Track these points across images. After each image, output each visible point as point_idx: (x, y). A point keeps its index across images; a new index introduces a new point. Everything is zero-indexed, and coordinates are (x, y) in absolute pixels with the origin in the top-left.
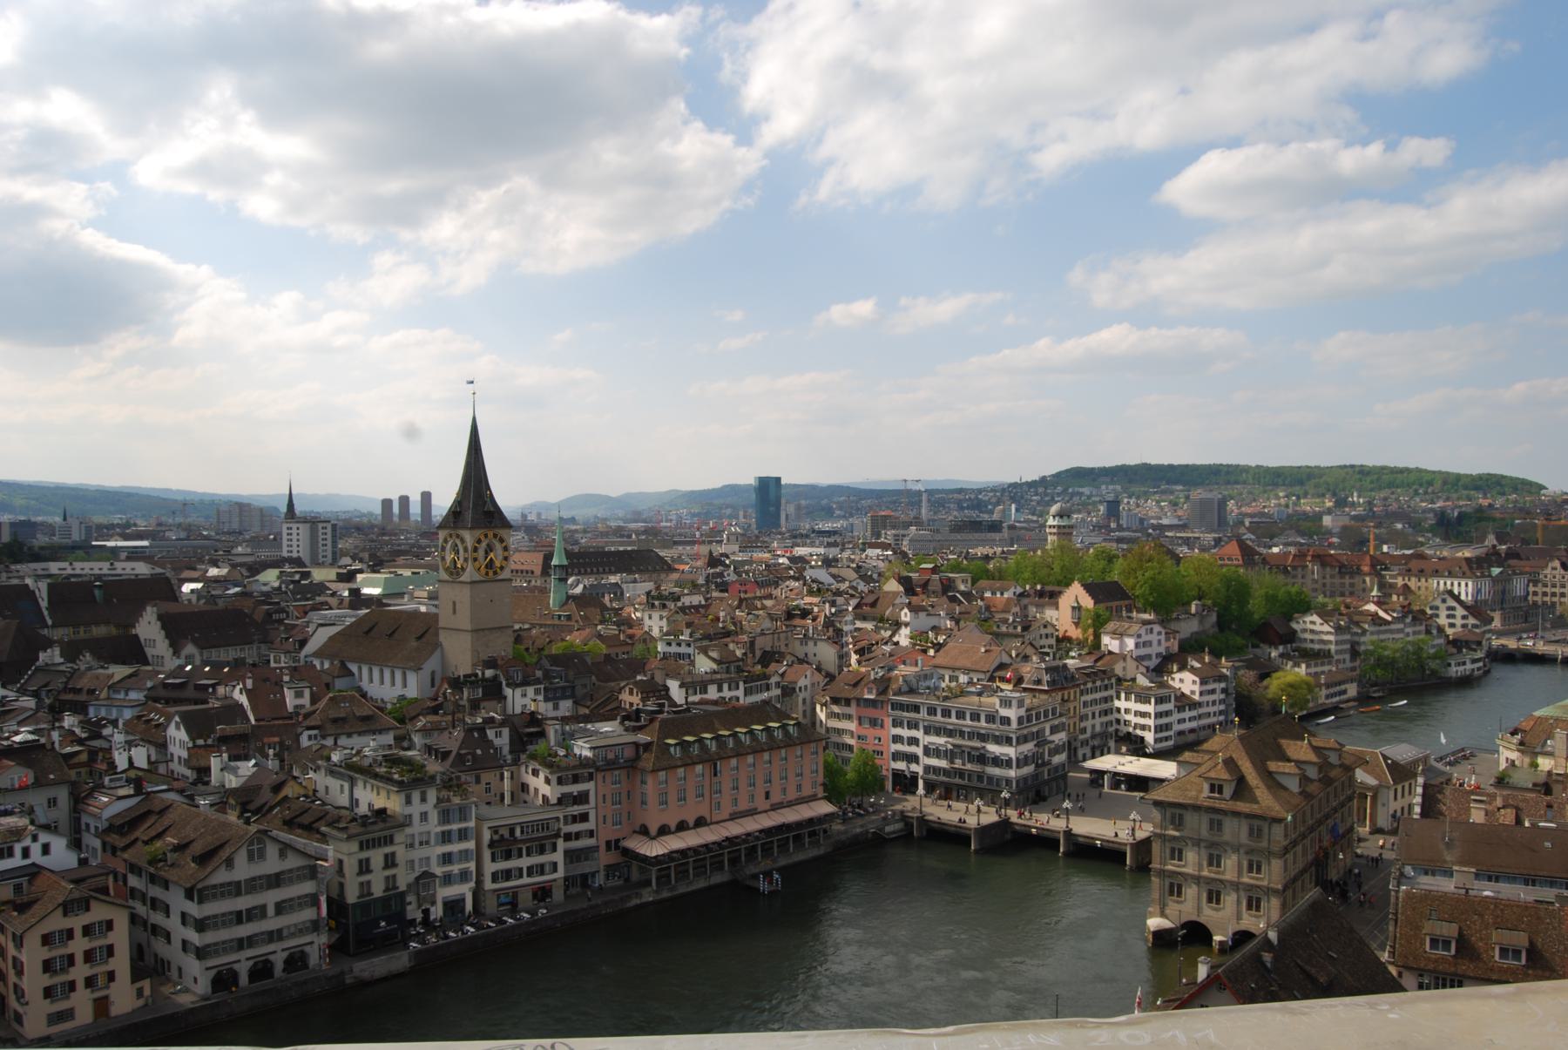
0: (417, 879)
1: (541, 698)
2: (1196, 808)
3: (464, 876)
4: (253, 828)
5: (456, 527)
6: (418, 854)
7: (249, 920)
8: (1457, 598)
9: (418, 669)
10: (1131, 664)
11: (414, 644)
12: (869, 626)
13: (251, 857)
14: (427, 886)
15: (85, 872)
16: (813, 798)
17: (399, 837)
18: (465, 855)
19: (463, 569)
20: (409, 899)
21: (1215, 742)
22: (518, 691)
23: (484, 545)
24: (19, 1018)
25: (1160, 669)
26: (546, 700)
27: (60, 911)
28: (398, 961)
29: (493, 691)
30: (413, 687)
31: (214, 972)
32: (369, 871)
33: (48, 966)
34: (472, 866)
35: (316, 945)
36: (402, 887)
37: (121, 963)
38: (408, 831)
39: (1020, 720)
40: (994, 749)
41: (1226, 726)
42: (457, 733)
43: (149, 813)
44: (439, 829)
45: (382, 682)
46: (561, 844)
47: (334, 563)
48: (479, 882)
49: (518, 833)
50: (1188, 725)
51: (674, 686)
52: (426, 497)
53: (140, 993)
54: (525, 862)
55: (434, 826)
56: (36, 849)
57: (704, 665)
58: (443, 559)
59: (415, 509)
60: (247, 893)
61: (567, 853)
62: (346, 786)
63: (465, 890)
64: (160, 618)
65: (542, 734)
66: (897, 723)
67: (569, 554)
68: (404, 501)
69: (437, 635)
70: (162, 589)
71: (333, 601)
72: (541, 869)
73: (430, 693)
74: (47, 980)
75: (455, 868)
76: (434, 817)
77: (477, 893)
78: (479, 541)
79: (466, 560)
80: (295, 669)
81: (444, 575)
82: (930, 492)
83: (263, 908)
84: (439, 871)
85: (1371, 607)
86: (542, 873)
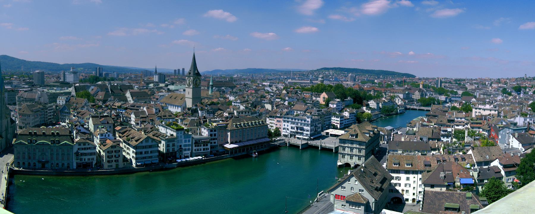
2: (348, 140)
3: (189, 149)
8: (400, 97)
9: (180, 106)
10: (335, 110)
12: (279, 100)
13: (146, 142)
15: (115, 141)
16: (265, 137)
21: (352, 126)
25: (341, 111)
30: (179, 110)
36: (176, 150)
39: (311, 122)
40: (305, 128)
41: (355, 123)
47: (164, 82)
48: (192, 151)
50: (347, 123)
51: (235, 112)
52: (183, 69)
57: (242, 108)
59: (181, 72)
64: (130, 93)
65: (206, 121)
66: (284, 121)
67: (213, 81)
68: (179, 70)
70: (131, 87)
75: (187, 148)
76: (183, 137)
81: (187, 86)
82: (293, 72)
85: (384, 99)
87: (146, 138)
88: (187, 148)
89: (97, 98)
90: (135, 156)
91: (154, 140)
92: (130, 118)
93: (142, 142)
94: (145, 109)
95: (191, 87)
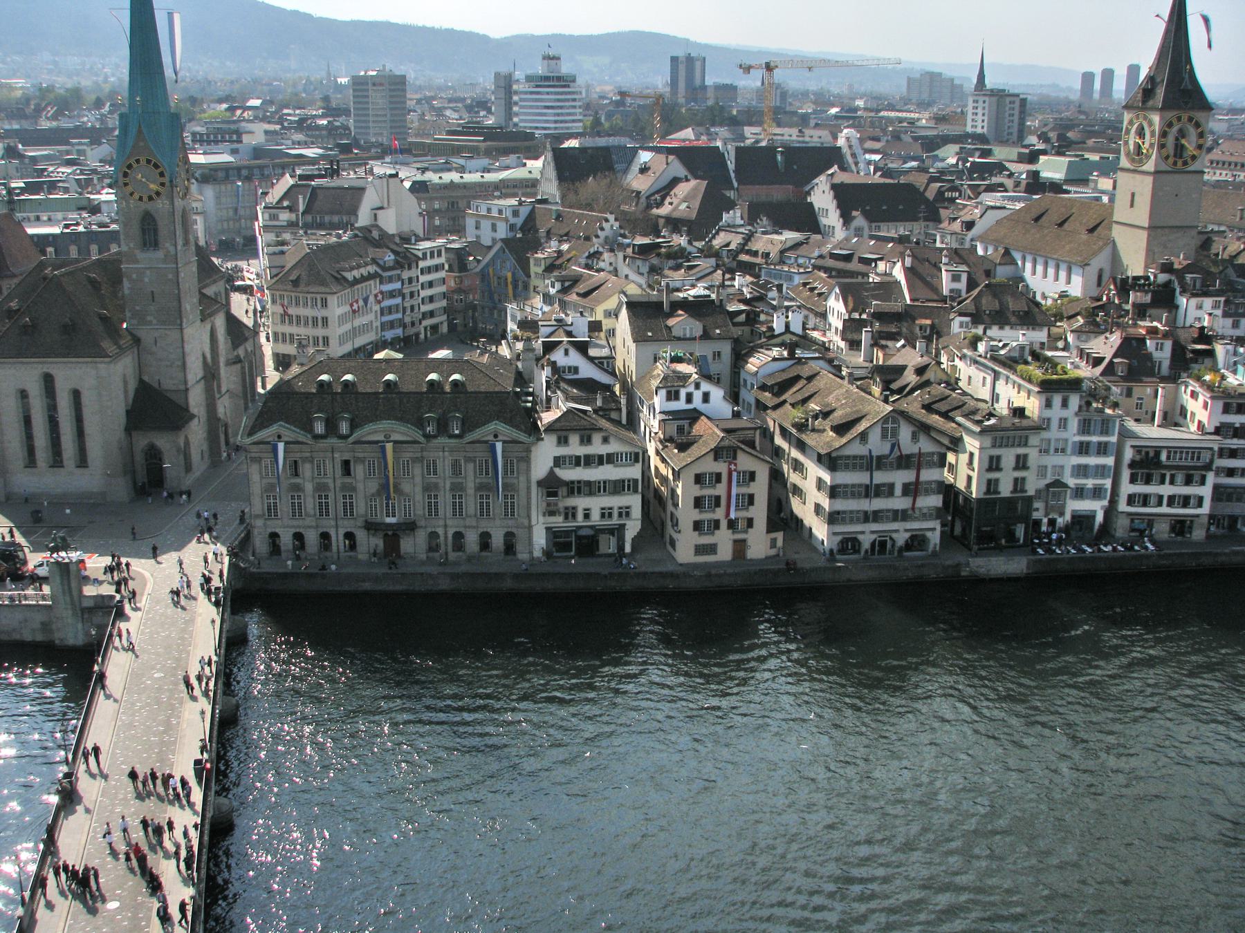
0: (1048, 486)
1: (1219, 312)
3: (1097, 493)
4: (890, 408)
5: (1144, 109)
6: (1052, 460)
7: (877, 495)
11: (1084, 236)
14: (1056, 496)
17: (1034, 440)
18: (1101, 471)
19: (1148, 157)
20: (1036, 505)
22: (1194, 302)
23: (1175, 129)
24: (673, 543)
26: (1225, 315)
27: (712, 455)
28: (1012, 565)
29: (1164, 298)
31: (839, 538)
32: (998, 469)
33: (698, 503)
34: (1108, 483)
35: (934, 532)
36: (1031, 492)
37: (759, 512)
38: (1045, 435)
42: (1115, 339)
43: (797, 378)
44: (1078, 438)
45: (1045, 276)
46: (1211, 478)
48: (1113, 501)
49: (1163, 457)
53: (773, 543)
54: (1166, 490)
55: (1073, 435)
56: (698, 396)
58: (1126, 143)
60: (594, 456)
61: (1216, 488)
62: (989, 379)
63: (1097, 507)
64: (834, 187)
65: (1211, 354)
69: (1110, 229)
71: (1009, 183)
72: (1185, 501)
73: (1095, 294)
74: (696, 515)
75: (1090, 483)
76: (1074, 424)
77: (1110, 511)
78: (1170, 125)
79: (1152, 145)
80: (956, 251)
83: (891, 486)
84: (1072, 482)
86: (1145, 504)
87: (885, 419)
88: (1090, 483)
89: (665, 210)
90: (826, 503)
91: (925, 428)
92: (823, 315)
93: (863, 436)
94: (898, 273)
95: (1150, 166)
